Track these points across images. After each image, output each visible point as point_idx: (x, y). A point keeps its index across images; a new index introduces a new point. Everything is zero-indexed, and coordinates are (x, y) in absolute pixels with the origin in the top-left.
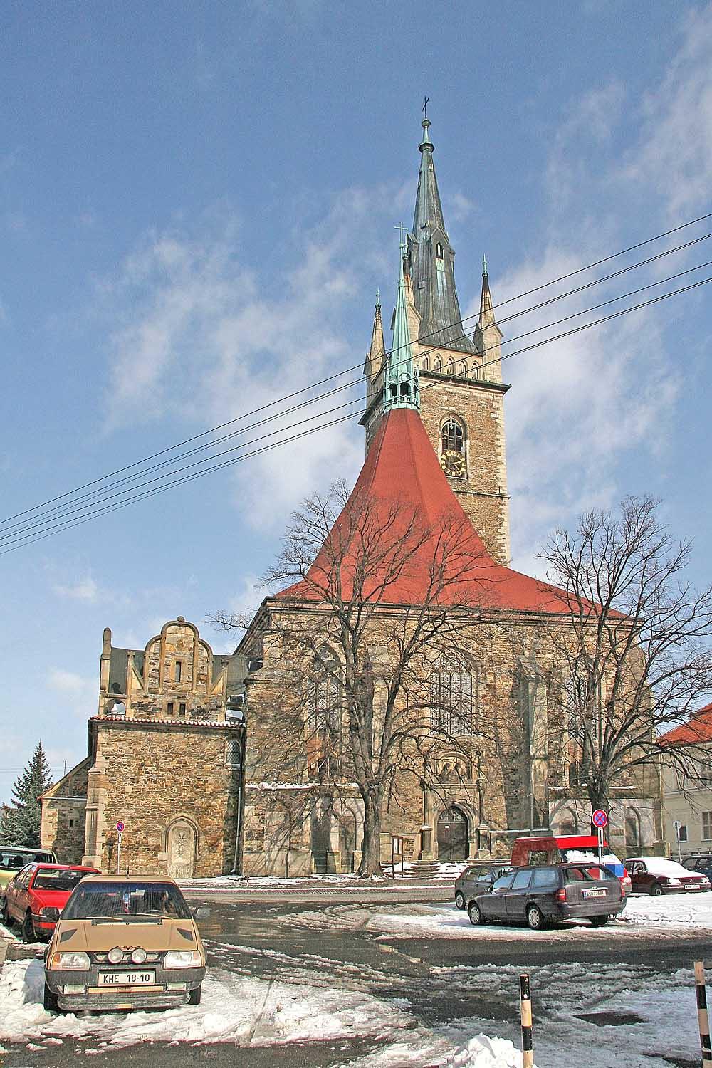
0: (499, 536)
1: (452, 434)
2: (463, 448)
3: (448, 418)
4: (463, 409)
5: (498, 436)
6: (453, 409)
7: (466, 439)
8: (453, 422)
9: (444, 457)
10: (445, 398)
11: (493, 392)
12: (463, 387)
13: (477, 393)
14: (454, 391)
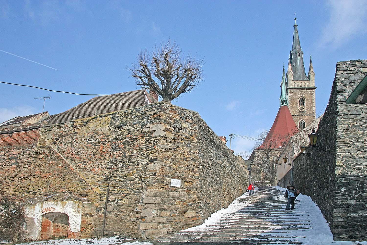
1: (301, 101)
2: (304, 104)
3: (300, 98)
4: (304, 95)
6: (302, 95)
7: (305, 102)
8: (302, 98)
9: (299, 107)
10: (300, 93)
13: (308, 90)
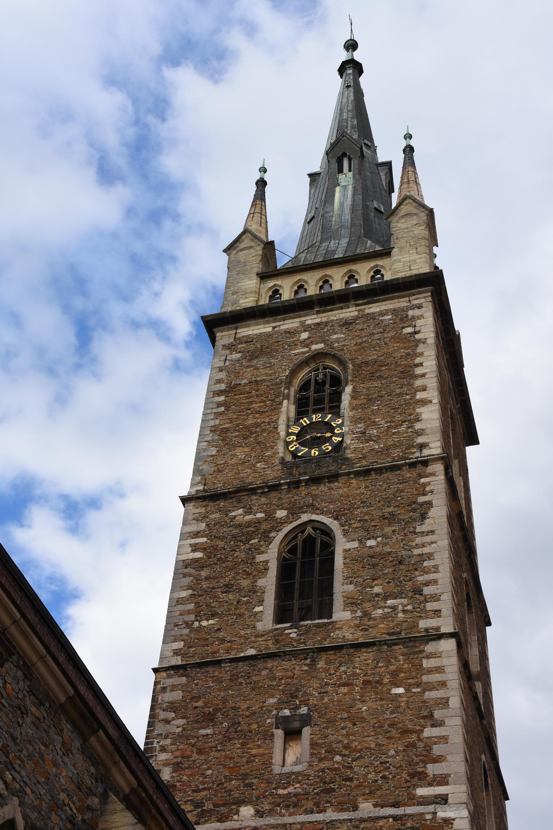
0: (419, 540)
5: (418, 360)
6: (321, 346)
10: (304, 335)
11: (409, 296)
12: (342, 308)
13: (374, 308)
14: (324, 320)
